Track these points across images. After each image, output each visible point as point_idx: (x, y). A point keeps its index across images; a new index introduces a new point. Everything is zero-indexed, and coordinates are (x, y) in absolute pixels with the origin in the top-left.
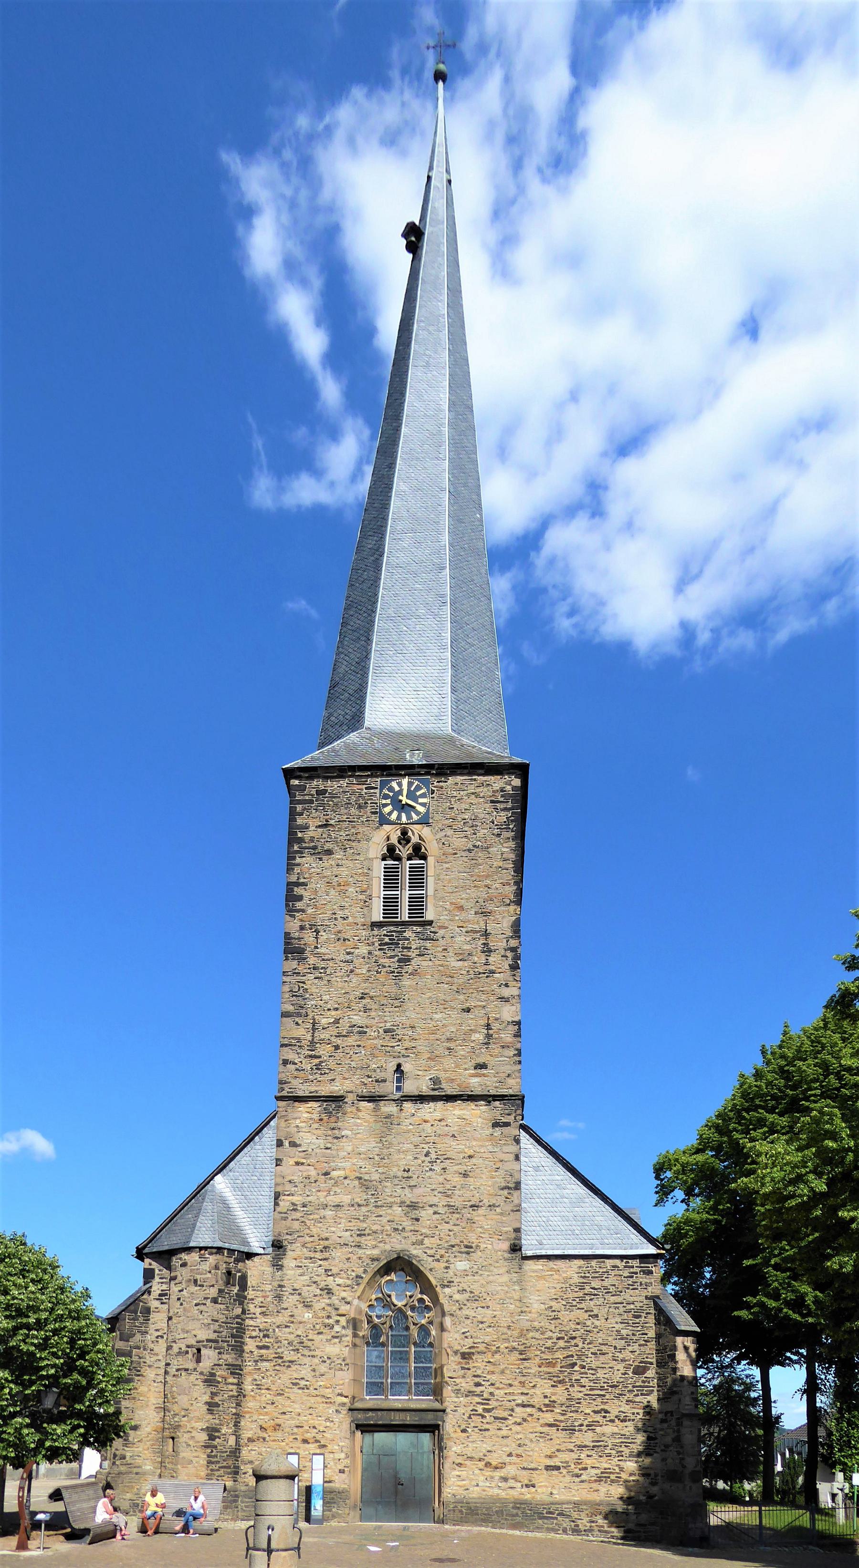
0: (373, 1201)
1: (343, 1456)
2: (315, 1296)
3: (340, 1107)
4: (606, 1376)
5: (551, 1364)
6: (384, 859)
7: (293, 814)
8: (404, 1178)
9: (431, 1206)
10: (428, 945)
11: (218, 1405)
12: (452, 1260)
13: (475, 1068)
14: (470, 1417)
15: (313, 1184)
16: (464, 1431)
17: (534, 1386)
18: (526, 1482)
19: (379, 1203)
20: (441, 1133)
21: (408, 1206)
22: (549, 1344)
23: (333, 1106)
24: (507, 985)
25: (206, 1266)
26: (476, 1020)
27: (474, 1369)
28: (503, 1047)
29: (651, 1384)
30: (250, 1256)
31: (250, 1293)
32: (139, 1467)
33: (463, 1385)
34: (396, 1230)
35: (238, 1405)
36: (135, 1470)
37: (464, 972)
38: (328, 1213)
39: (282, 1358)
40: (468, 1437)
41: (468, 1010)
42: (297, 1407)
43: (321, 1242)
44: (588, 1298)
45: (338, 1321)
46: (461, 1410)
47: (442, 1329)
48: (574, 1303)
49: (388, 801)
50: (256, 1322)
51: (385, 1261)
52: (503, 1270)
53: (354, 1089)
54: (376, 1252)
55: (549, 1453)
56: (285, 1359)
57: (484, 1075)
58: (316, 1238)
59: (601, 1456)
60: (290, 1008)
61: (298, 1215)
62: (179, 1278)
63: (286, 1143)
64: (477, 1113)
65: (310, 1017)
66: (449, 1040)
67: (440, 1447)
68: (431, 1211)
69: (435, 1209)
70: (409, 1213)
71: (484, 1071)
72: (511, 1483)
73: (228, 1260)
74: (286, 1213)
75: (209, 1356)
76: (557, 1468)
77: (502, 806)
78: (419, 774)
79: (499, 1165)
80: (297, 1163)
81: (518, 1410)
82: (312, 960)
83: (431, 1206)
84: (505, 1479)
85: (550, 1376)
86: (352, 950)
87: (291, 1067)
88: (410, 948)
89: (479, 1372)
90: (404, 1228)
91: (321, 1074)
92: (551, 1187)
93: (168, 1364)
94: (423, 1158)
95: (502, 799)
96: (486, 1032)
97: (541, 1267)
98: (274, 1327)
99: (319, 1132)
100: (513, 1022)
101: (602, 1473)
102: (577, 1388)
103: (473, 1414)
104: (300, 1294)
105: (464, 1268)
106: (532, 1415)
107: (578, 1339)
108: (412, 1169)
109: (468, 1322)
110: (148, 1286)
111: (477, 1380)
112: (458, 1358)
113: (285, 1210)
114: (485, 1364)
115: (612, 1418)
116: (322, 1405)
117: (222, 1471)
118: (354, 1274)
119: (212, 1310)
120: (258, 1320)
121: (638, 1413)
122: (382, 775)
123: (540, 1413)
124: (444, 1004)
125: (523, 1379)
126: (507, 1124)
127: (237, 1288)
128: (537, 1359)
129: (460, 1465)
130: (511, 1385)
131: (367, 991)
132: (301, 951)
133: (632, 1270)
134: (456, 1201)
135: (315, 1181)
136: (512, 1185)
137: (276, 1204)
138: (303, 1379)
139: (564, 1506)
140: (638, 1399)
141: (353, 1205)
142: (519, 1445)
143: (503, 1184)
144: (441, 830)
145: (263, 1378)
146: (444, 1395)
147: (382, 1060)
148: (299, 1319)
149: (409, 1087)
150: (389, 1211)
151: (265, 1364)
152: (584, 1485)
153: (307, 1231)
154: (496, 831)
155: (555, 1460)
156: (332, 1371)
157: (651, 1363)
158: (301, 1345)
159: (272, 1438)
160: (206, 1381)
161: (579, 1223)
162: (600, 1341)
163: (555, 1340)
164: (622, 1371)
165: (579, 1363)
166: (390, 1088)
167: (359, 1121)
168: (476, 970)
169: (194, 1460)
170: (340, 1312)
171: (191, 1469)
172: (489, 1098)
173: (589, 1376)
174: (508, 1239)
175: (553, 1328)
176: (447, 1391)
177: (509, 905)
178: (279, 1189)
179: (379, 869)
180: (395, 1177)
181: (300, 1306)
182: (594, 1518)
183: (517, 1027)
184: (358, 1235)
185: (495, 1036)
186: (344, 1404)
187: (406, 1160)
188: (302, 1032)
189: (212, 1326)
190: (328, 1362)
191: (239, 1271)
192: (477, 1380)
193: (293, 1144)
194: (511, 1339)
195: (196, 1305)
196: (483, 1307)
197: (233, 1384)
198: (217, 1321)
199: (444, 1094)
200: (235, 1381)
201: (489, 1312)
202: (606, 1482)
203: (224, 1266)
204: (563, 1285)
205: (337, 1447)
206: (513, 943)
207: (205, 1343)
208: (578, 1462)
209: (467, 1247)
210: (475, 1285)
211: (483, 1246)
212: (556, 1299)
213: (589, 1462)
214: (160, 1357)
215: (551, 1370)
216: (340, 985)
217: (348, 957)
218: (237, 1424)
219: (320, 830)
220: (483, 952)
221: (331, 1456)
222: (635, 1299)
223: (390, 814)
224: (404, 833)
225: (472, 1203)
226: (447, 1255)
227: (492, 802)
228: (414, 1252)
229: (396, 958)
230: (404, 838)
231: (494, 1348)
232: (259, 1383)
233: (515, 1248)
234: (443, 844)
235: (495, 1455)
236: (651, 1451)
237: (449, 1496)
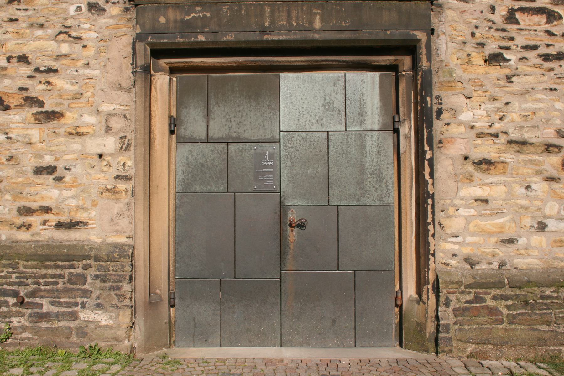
14: (511, 18)
40: (509, 78)
103: (522, 10)
221: (76, 145)
237: (453, 262)
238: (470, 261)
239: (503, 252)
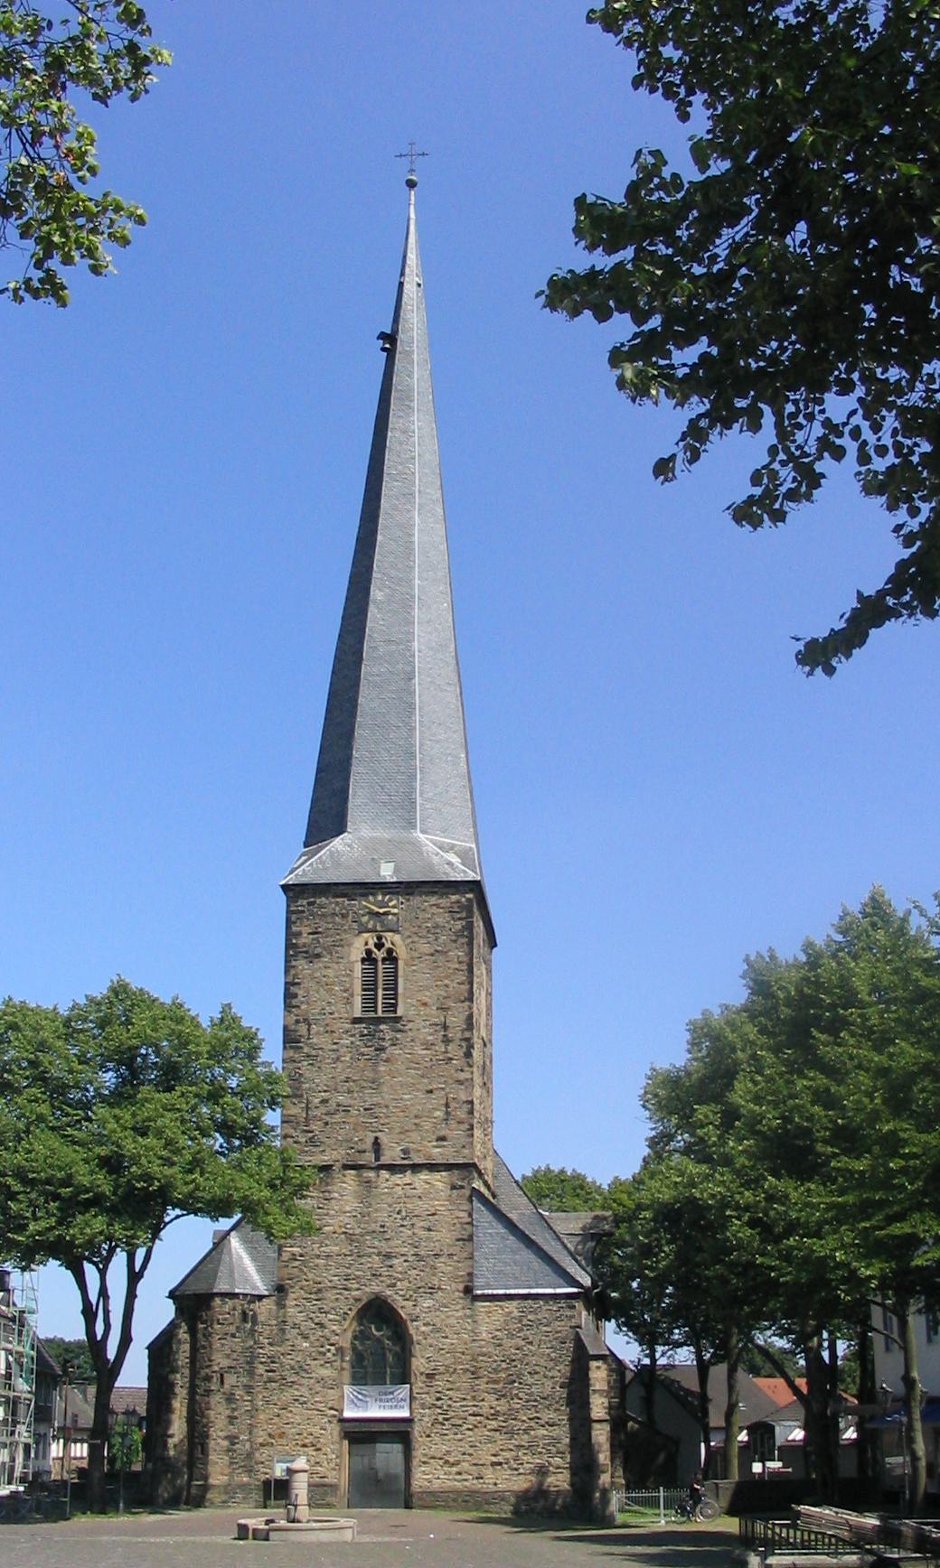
1: (334, 1456)
5: (496, 1382)
7: (289, 923)
10: (398, 1036)
12: (419, 1299)
13: (437, 1140)
16: (429, 1436)
18: (476, 1475)
22: (494, 1365)
24: (462, 1070)
26: (437, 1100)
28: (459, 1122)
31: (259, 1328)
34: (374, 1275)
41: (431, 1092)
42: (298, 1419)
45: (329, 1350)
53: (340, 1158)
57: (444, 1146)
64: (439, 1180)
77: (459, 916)
82: (306, 1050)
85: (495, 1391)
89: (440, 1389)
94: (396, 1216)
102: (516, 1401)
106: (480, 1423)
111: (438, 1395)
112: (424, 1378)
113: (286, 1259)
117: (240, 1471)
125: (474, 1394)
126: (462, 1187)
129: (424, 1463)
130: (464, 1399)
137: (280, 1255)
144: (410, 937)
149: (385, 1160)
152: (521, 1477)
154: (454, 938)
158: (300, 1369)
164: (551, 1385)
166: (369, 1157)
170: (332, 1342)
172: (449, 1167)
180: (374, 1232)
181: (299, 1337)
186: (334, 1416)
187: (382, 1216)
192: (438, 1395)
206: (467, 1035)
209: (430, 1288)
215: (496, 1386)
217: (335, 1047)
224: (379, 938)
228: (389, 1293)
231: (451, 1370)
233: (468, 1290)
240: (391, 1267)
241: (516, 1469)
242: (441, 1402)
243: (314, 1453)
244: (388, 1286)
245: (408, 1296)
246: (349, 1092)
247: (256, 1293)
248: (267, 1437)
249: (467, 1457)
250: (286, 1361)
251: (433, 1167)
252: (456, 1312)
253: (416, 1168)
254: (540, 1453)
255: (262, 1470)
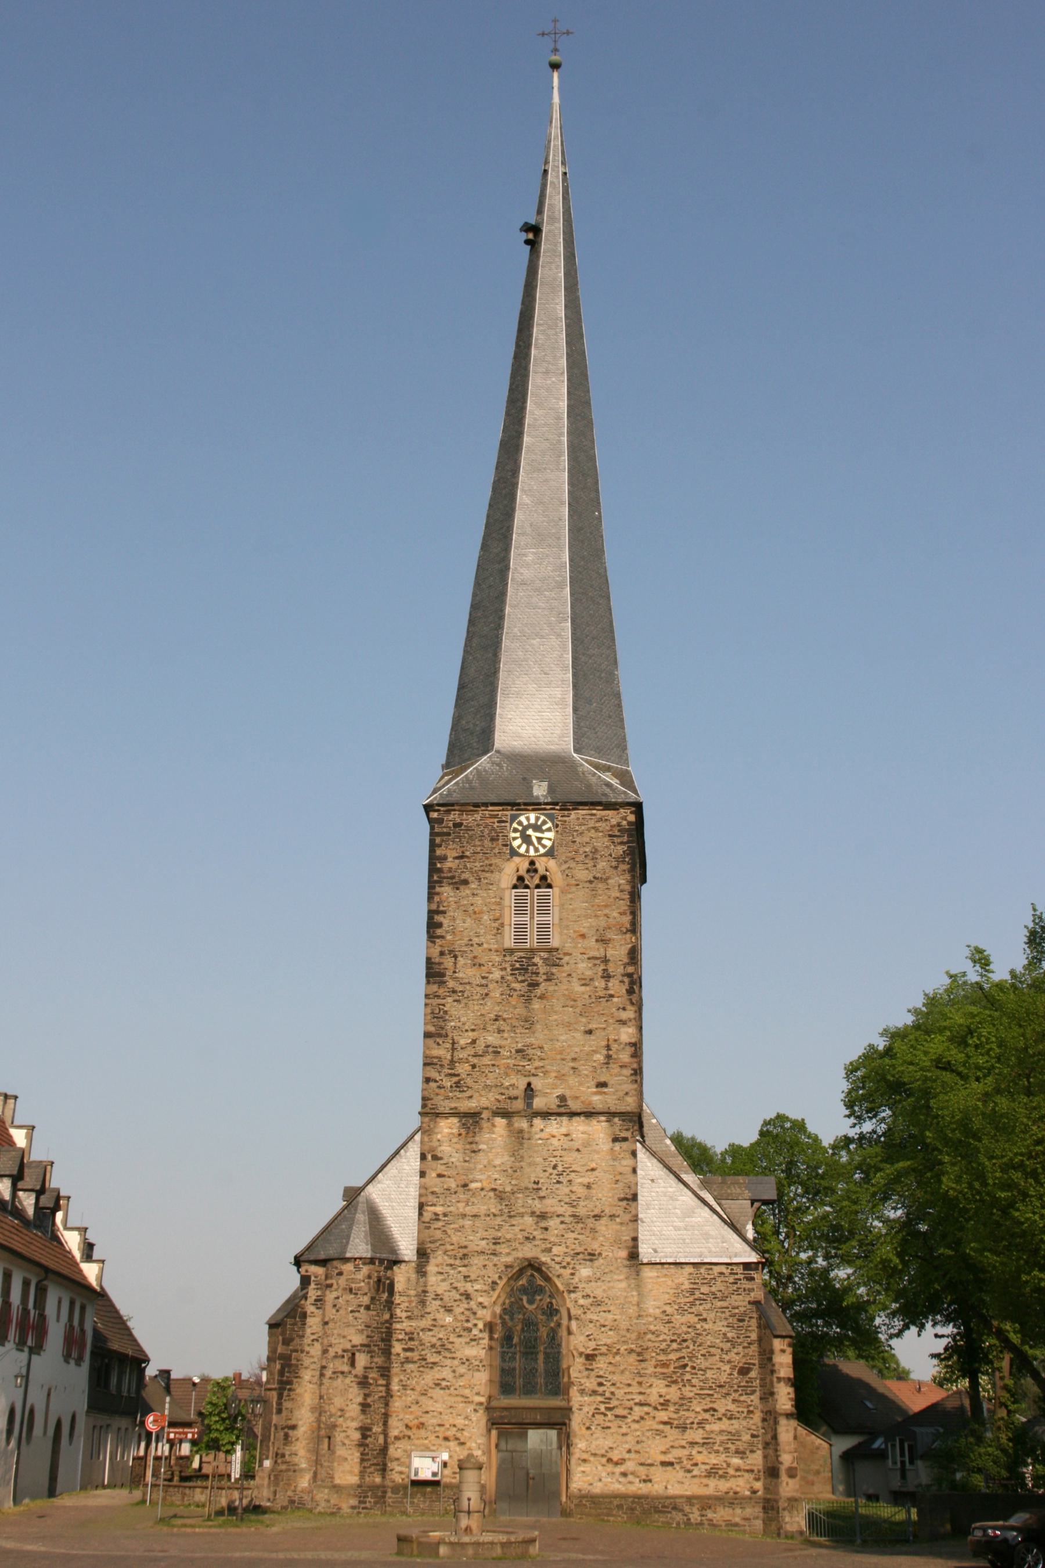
0: (506, 1211)
2: (455, 1301)
3: (477, 1122)
4: (714, 1377)
5: (665, 1365)
6: (515, 887)
7: (433, 846)
8: (534, 1189)
9: (558, 1216)
11: (369, 1406)
12: (577, 1267)
13: (597, 1086)
14: (593, 1416)
15: (454, 1196)
16: (588, 1428)
17: (651, 1386)
18: (644, 1477)
19: (512, 1213)
20: (567, 1147)
21: (538, 1216)
22: (663, 1346)
23: (471, 1121)
24: (624, 1009)
25: (360, 1276)
26: (597, 1041)
27: (597, 1370)
28: (621, 1067)
29: (754, 1384)
30: (397, 1262)
31: (397, 1299)
32: (296, 1465)
33: (587, 1385)
34: (527, 1238)
35: (387, 1405)
36: (292, 1468)
37: (587, 997)
38: (468, 1223)
39: (425, 1360)
40: (592, 1435)
42: (439, 1407)
43: (461, 1250)
44: (698, 1302)
46: (586, 1409)
47: (570, 1333)
48: (686, 1308)
49: (518, 835)
50: (402, 1326)
51: (518, 1268)
52: (622, 1277)
54: (509, 1260)
55: (664, 1449)
56: (429, 1360)
58: (456, 1246)
59: (710, 1453)
60: (432, 1029)
61: (440, 1224)
62: (335, 1286)
63: (429, 1157)
64: (599, 1130)
65: (450, 1037)
66: (574, 1059)
67: (566, 1441)
68: (558, 1220)
69: (561, 1219)
70: (538, 1222)
71: (605, 1090)
72: (631, 1478)
73: (378, 1269)
74: (429, 1223)
75: (362, 1360)
76: (671, 1464)
78: (545, 809)
79: (618, 1178)
80: (440, 1176)
81: (636, 1409)
82: (451, 984)
83: (558, 1216)
84: (624, 1474)
86: (487, 975)
87: (433, 1085)
88: (538, 973)
89: (601, 1373)
90: (534, 1237)
91: (460, 1091)
92: (665, 1199)
93: (323, 1367)
94: (550, 1170)
95: (618, 834)
96: (606, 1052)
97: (656, 1274)
98: (418, 1330)
99: (458, 1146)
100: (630, 1043)
101: (711, 1469)
102: (688, 1388)
104: (441, 1299)
105: (588, 1274)
106: (648, 1413)
107: (690, 1341)
108: (542, 1181)
109: (591, 1325)
110: (304, 1291)
112: (582, 1360)
114: (606, 1365)
115: (720, 1416)
116: (461, 1405)
117: (372, 1469)
118: (490, 1280)
119: (363, 1314)
120: (404, 1324)
121: (743, 1412)
122: (512, 810)
123: (656, 1412)
124: (569, 1026)
125: (641, 1379)
127: (386, 1294)
128: (654, 1360)
129: (585, 1461)
130: (629, 1385)
131: (500, 1014)
132: (443, 975)
133: (736, 1277)
134: (582, 1211)
135: (456, 1193)
136: (630, 1197)
137: (420, 1214)
138: (444, 1379)
139: (677, 1500)
140: (742, 1398)
141: (489, 1215)
142: (638, 1442)
143: (622, 1196)
144: (566, 862)
145: (408, 1379)
146: (571, 1395)
147: (513, 1079)
148: (441, 1323)
149: (538, 1103)
150: (521, 1221)
151: (411, 1366)
152: (696, 1480)
153: (448, 1239)
154: (614, 864)
155: (669, 1456)
156: (471, 1372)
157: (754, 1364)
158: (442, 1348)
159: (417, 1436)
160: (359, 1383)
161: (689, 1233)
162: (709, 1343)
163: (669, 1343)
164: (728, 1371)
165: (690, 1364)
166: (519, 1105)
167: (494, 1136)
168: (597, 994)
169: (349, 1458)
171: (346, 1466)
172: (610, 1115)
173: (699, 1376)
174: (627, 1247)
175: (666, 1331)
176: (574, 1391)
177: (626, 933)
178: (423, 1200)
179: (510, 897)
180: (527, 1188)
182: (704, 1512)
183: (633, 1048)
184: (495, 1244)
185: (614, 1056)
186: (481, 1404)
188: (441, 1052)
189: (365, 1332)
190: (467, 1363)
191: (388, 1278)
193: (435, 1158)
194: (630, 1342)
195: (352, 1312)
196: (605, 1312)
197: (382, 1385)
198: (369, 1327)
199: (568, 1111)
200: (384, 1382)
201: (610, 1316)
202: (715, 1477)
203: (376, 1274)
204: (676, 1291)
205: (474, 1445)
206: (630, 969)
207: (359, 1348)
208: (690, 1457)
210: (598, 1290)
211: (604, 1254)
212: (670, 1304)
213: (699, 1458)
214: (315, 1360)
216: (476, 1008)
217: (484, 982)
218: (385, 1424)
219: (457, 861)
220: (603, 977)
222: (740, 1303)
223: (519, 847)
224: (532, 863)
225: (596, 1213)
226: (573, 1262)
227: (610, 836)
228: (543, 1259)
229: (526, 983)
230: (532, 868)
231: (615, 1350)
232: (404, 1383)
233: (633, 1255)
234: (567, 875)
235: (616, 1452)
236: (755, 1449)
238: (580, 1490)
239: (590, 1488)
240: (546, 1229)
241: (689, 1471)
242: (604, 1388)
243: (458, 1449)
244: (543, 1251)
245: (564, 1264)
246: (500, 1031)
247: (394, 1258)
248: (404, 1429)
249: (633, 1455)
250: (427, 1338)
251: (589, 1114)
252: (619, 1284)
253: (573, 1114)
254: (717, 1452)
255: (398, 1469)
